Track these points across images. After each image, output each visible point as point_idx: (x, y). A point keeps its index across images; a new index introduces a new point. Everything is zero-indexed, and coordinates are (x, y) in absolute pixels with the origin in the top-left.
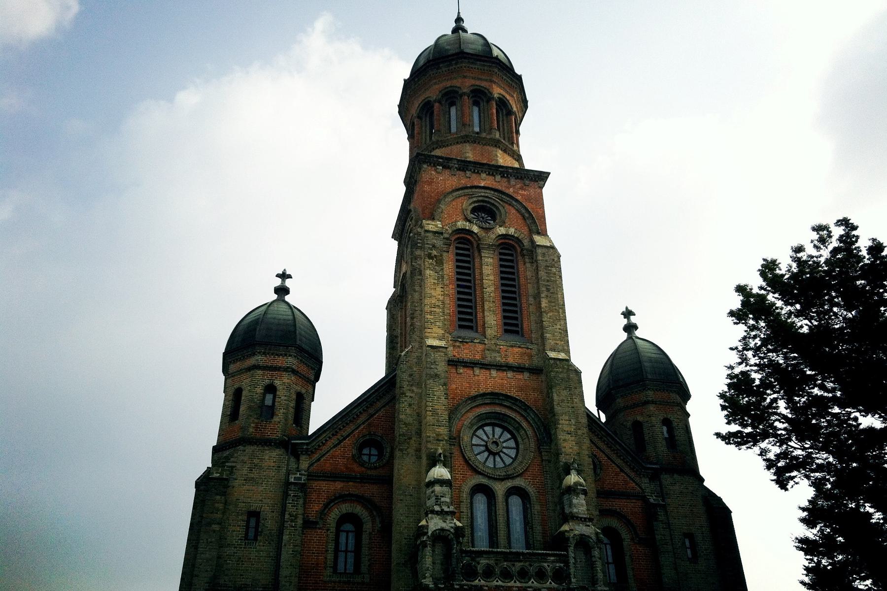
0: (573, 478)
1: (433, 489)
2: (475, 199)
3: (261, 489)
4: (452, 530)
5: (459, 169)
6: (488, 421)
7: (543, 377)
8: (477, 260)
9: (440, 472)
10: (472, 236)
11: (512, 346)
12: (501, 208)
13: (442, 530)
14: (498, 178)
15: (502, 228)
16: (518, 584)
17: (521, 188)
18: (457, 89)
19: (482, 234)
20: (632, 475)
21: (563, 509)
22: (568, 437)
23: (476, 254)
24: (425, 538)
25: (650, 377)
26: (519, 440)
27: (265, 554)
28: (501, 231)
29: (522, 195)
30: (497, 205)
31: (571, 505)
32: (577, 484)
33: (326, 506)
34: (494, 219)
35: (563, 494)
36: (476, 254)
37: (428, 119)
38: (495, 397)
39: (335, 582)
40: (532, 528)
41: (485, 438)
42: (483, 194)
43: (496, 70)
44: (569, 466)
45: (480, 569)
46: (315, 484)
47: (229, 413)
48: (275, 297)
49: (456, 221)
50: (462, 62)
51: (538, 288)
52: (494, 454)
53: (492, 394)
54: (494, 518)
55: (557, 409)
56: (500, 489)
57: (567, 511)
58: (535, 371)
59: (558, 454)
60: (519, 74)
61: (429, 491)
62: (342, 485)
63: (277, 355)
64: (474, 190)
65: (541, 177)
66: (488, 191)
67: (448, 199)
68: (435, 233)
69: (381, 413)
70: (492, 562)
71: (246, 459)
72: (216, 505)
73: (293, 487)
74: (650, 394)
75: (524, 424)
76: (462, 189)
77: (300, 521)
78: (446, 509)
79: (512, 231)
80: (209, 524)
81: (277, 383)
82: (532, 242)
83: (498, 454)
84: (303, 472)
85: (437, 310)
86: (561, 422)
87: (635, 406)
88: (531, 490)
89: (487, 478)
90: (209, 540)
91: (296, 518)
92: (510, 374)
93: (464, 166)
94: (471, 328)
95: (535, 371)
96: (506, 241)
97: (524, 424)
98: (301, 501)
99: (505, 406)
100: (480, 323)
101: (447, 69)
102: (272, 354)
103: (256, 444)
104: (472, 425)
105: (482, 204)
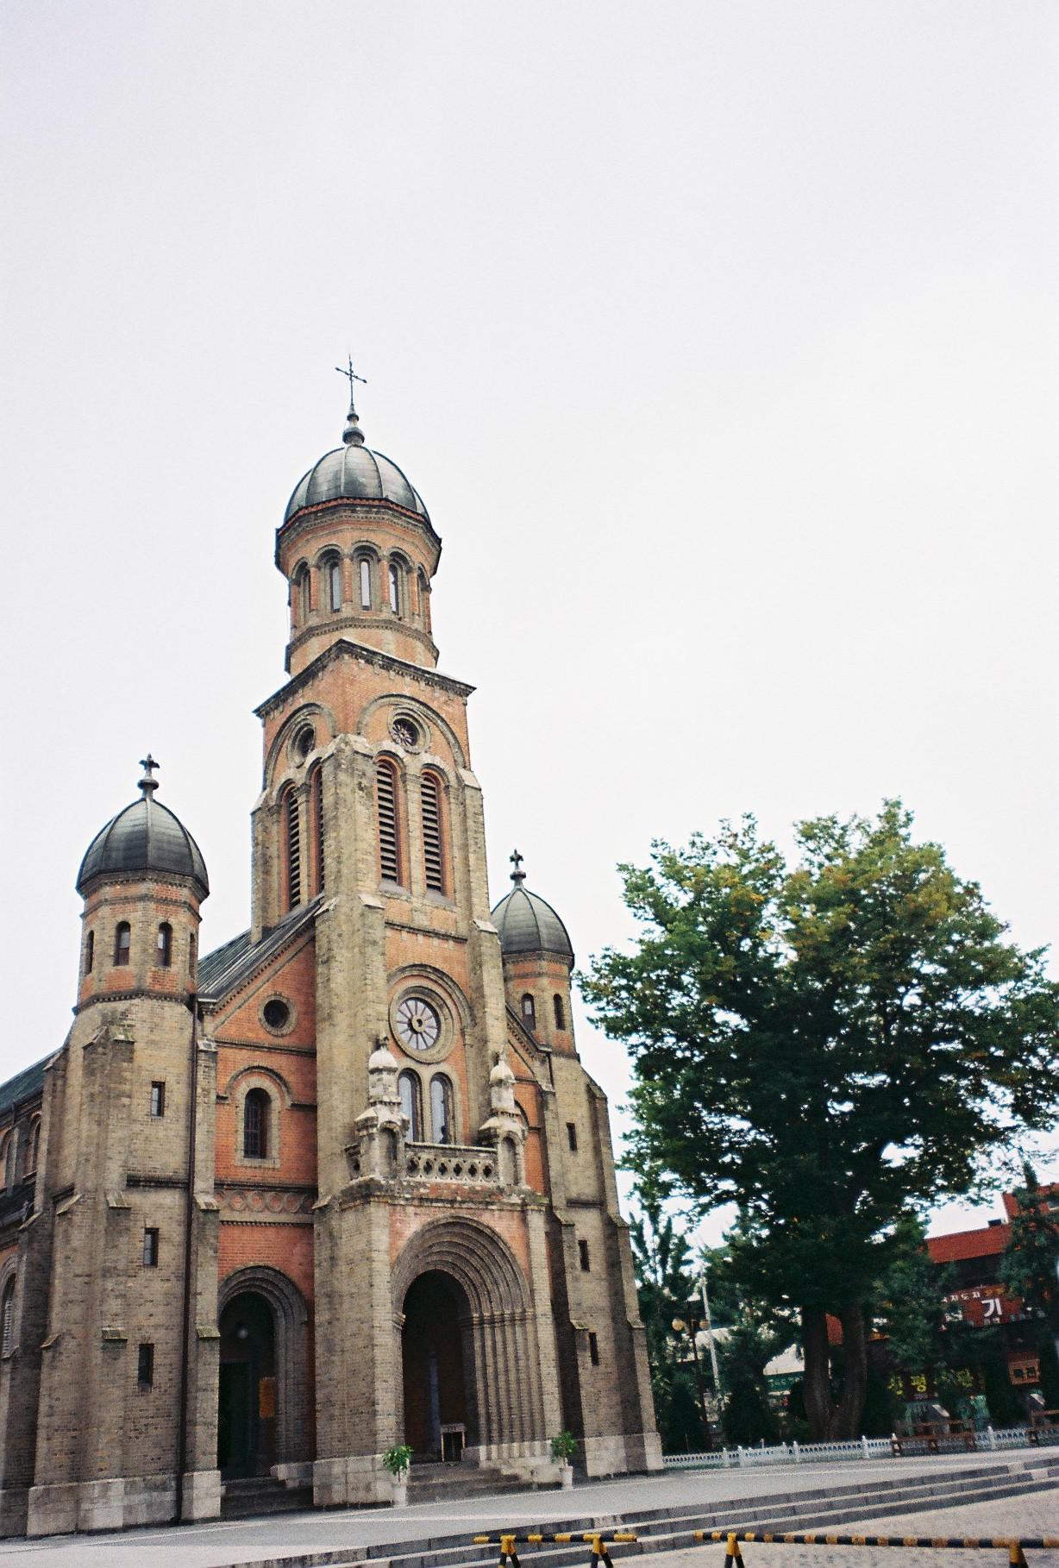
0: (502, 1071)
1: (380, 1076)
2: (399, 711)
3: (164, 1055)
4: (399, 1123)
5: (382, 667)
6: (413, 995)
7: (466, 948)
8: (401, 793)
9: (385, 1058)
10: (396, 761)
11: (437, 907)
12: (425, 727)
13: (390, 1122)
14: (423, 684)
15: (427, 755)
16: (454, 1181)
17: (446, 702)
18: (375, 547)
19: (407, 758)
20: (526, 1057)
21: (489, 1102)
22: (496, 1022)
24: (375, 1130)
25: (546, 947)
26: (442, 1018)
27: (173, 1133)
28: (427, 758)
29: (447, 713)
30: (421, 721)
31: (500, 1099)
32: (508, 1077)
33: (235, 1078)
34: (414, 742)
35: (492, 1086)
36: (400, 785)
37: (328, 571)
38: (422, 968)
39: (246, 1167)
40: (453, 1118)
41: (409, 1015)
42: (408, 706)
43: (421, 531)
44: (498, 1056)
45: (422, 1164)
46: (226, 1052)
47: (112, 953)
48: (139, 793)
49: (382, 740)
50: (384, 513)
51: (467, 839)
52: (416, 1032)
53: (421, 965)
54: (419, 1106)
55: (487, 991)
56: (426, 1073)
57: (495, 1104)
58: (460, 940)
59: (484, 1041)
60: (440, 536)
61: (375, 1077)
62: (250, 1053)
63: (170, 884)
64: (398, 699)
66: (413, 703)
67: (373, 707)
68: (365, 755)
69: (286, 969)
70: (431, 1157)
71: (146, 1016)
72: (125, 1074)
73: (202, 1056)
74: (544, 965)
75: (449, 1002)
76: (387, 696)
77: (213, 1097)
78: (394, 1101)
79: (437, 761)
80: (119, 1096)
81: (173, 921)
82: (458, 778)
83: (416, 1032)
84: (209, 1037)
85: (370, 858)
86: (489, 1005)
87: (525, 976)
88: (454, 1077)
89: (414, 1062)
90: (120, 1116)
91: (209, 1093)
92: (436, 942)
93: (389, 664)
94: (393, 878)
95: (460, 940)
96: (430, 771)
97: (449, 1002)
98: (213, 1073)
99: (432, 980)
100: (405, 874)
101: (364, 515)
102: (166, 882)
103: (155, 997)
104: (399, 998)
105: (403, 717)
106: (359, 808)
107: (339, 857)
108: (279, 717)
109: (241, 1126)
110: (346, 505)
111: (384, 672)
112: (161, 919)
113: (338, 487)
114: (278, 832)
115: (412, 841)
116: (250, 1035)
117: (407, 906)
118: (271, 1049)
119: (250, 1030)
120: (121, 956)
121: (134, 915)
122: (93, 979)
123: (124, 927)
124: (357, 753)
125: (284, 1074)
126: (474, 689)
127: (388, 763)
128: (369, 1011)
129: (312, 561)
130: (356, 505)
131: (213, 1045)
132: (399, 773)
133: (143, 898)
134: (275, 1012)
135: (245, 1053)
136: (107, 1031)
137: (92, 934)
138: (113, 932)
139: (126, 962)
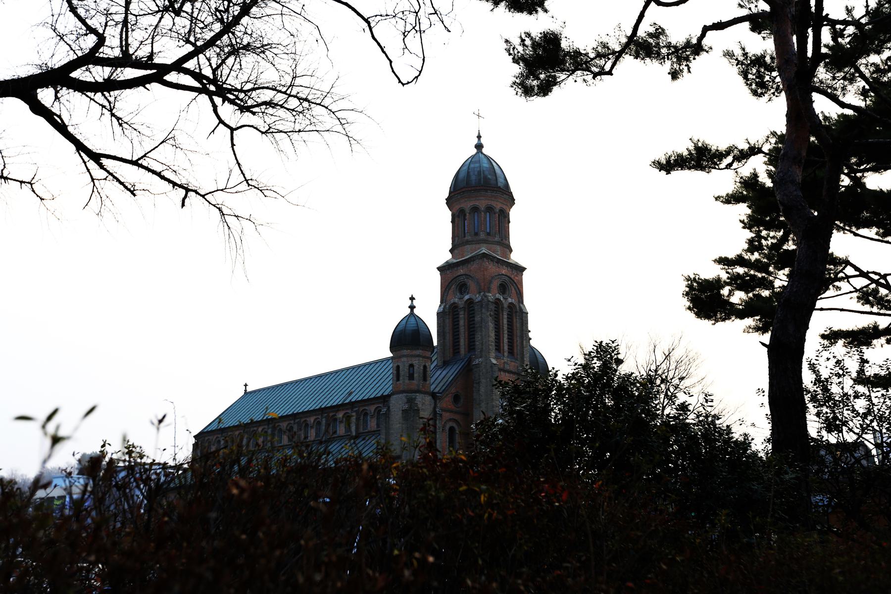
5: (496, 262)
8: (501, 315)
12: (509, 287)
23: (501, 311)
28: (510, 300)
46: (444, 414)
47: (408, 375)
65: (522, 269)
73: (438, 415)
77: (441, 430)
106: (490, 324)
107: (482, 343)
108: (450, 275)
109: (448, 440)
110: (485, 190)
111: (497, 264)
112: (424, 364)
113: (480, 180)
114: (449, 321)
115: (505, 335)
116: (450, 407)
117: (503, 361)
118: (456, 413)
119: (450, 405)
120: (411, 377)
121: (415, 362)
122: (400, 384)
123: (411, 366)
124: (489, 301)
125: (459, 421)
126: (526, 269)
127: (497, 302)
128: (494, 404)
129: (467, 211)
130: (487, 190)
131: (440, 411)
132: (500, 307)
133: (418, 356)
134: (456, 398)
135: (448, 414)
136: (411, 405)
137: (398, 367)
138: (408, 368)
139: (413, 380)
